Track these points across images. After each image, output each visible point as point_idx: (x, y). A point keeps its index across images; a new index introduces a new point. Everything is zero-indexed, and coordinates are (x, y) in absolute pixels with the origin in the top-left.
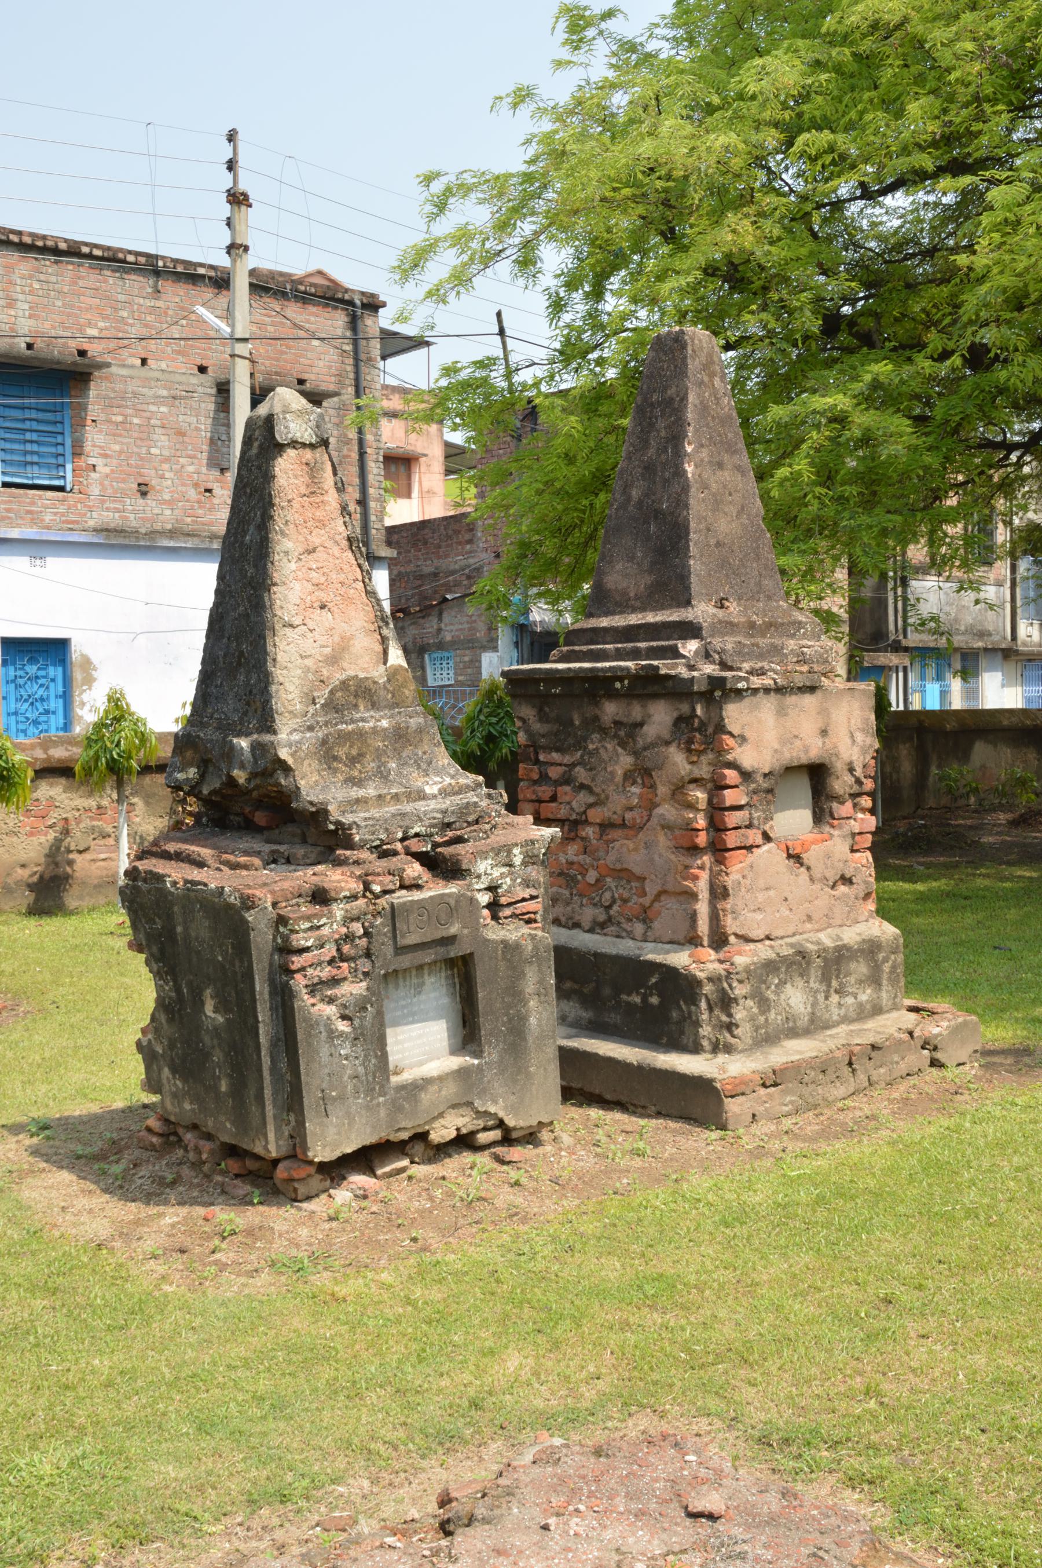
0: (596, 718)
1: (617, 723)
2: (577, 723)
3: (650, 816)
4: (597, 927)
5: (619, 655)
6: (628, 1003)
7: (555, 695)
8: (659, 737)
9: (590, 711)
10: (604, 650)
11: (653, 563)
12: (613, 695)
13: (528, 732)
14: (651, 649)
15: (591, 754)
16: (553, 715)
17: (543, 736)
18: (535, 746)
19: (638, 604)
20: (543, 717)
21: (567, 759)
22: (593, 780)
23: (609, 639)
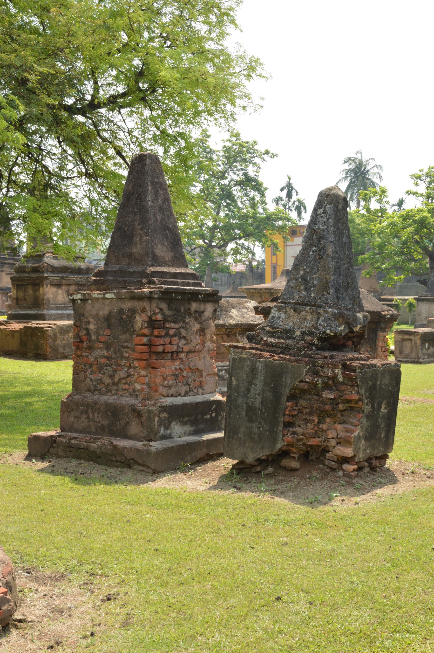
0: (189, 309)
1: (196, 311)
2: (182, 311)
3: (204, 347)
4: (186, 394)
5: (183, 284)
6: (206, 419)
7: (178, 299)
8: (208, 317)
9: (187, 306)
10: (178, 282)
11: (172, 248)
12: (197, 300)
13: (163, 314)
14: (193, 283)
15: (186, 323)
16: (174, 307)
17: (169, 316)
18: (165, 320)
19: (170, 264)
20: (170, 308)
21: (177, 326)
22: (187, 334)
23: (168, 277)
